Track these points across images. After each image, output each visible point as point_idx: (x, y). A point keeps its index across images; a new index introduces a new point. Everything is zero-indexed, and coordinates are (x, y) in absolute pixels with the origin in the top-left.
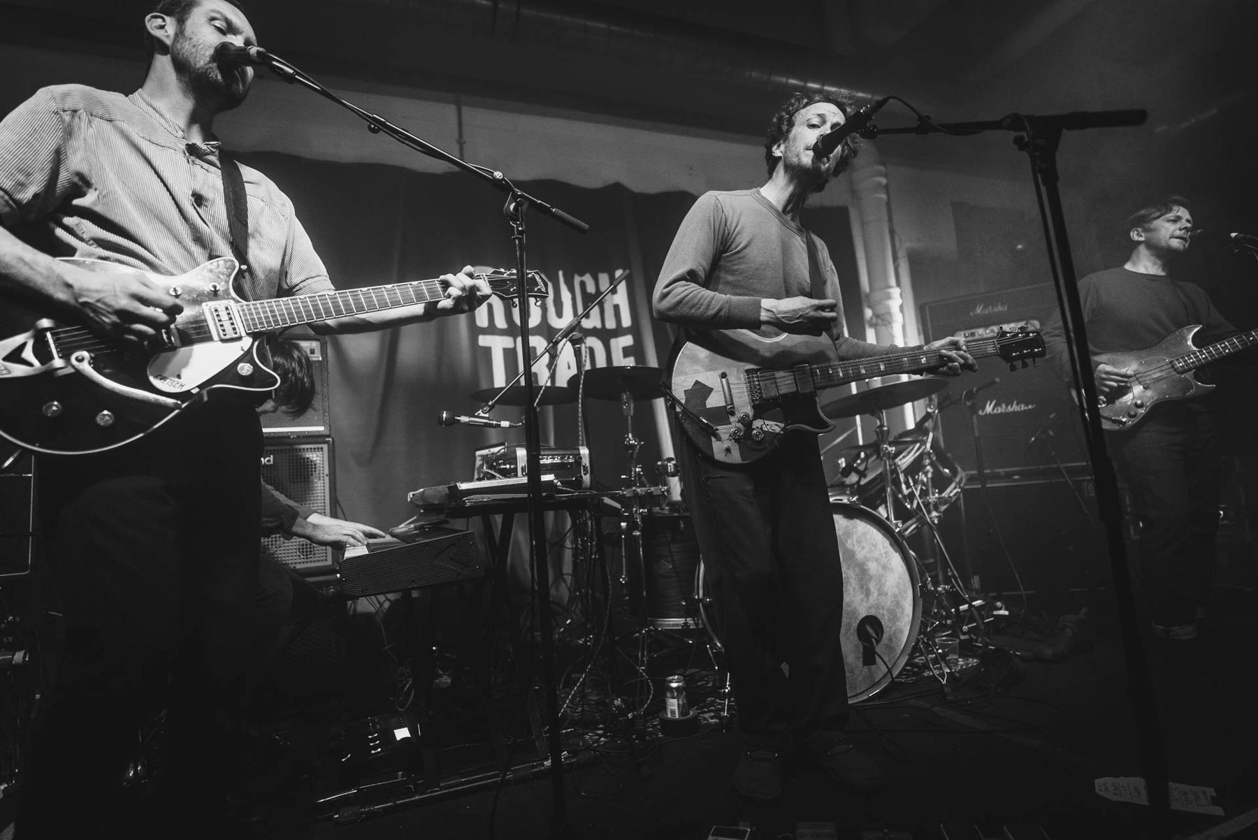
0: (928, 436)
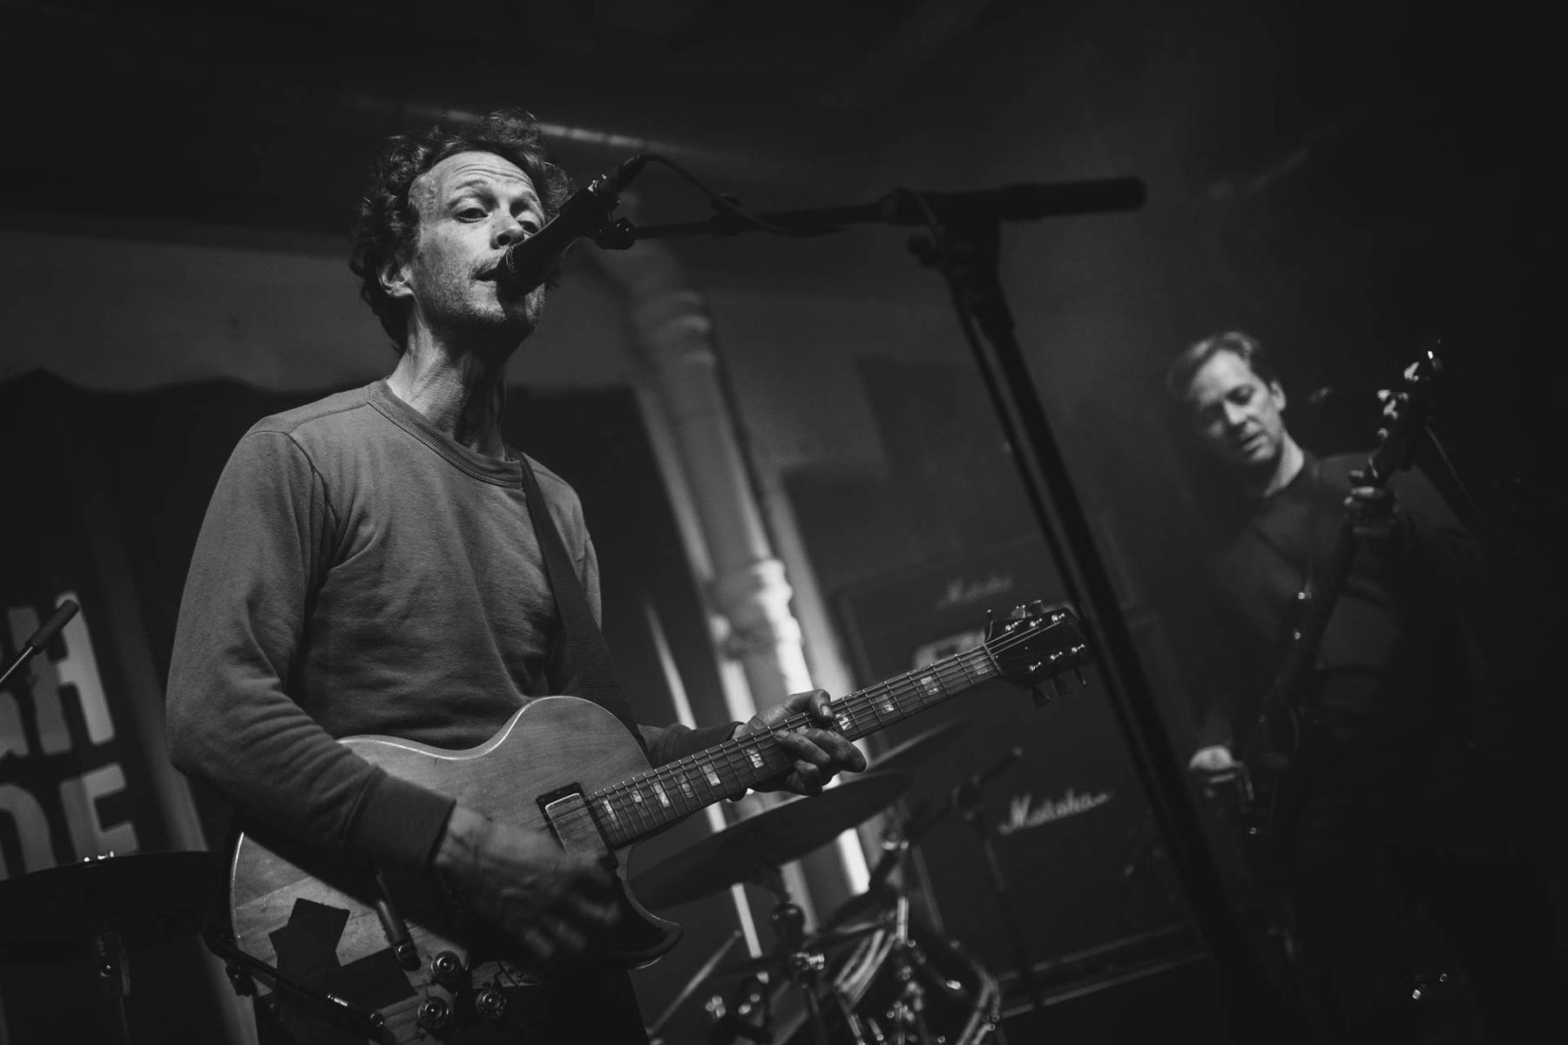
0: (895, 906)
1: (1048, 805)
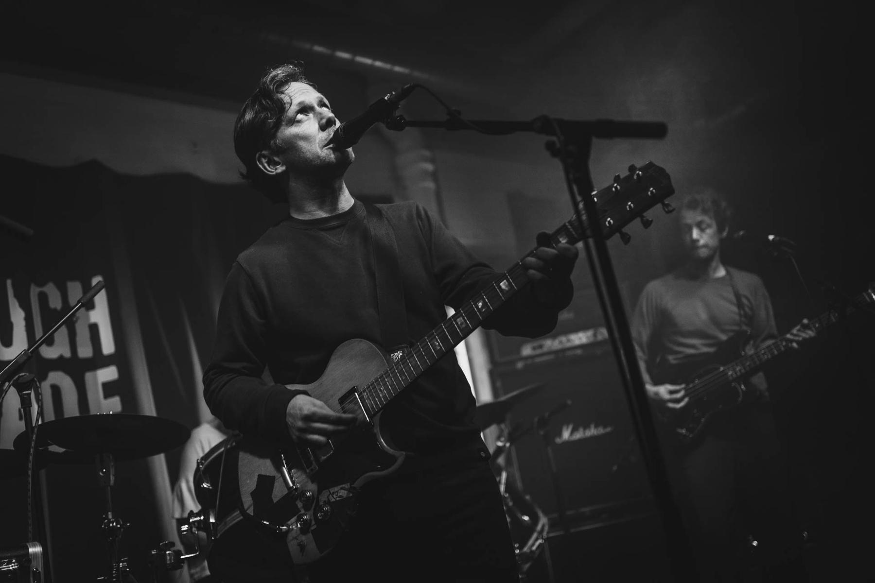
0: (500, 475)
1: (581, 430)
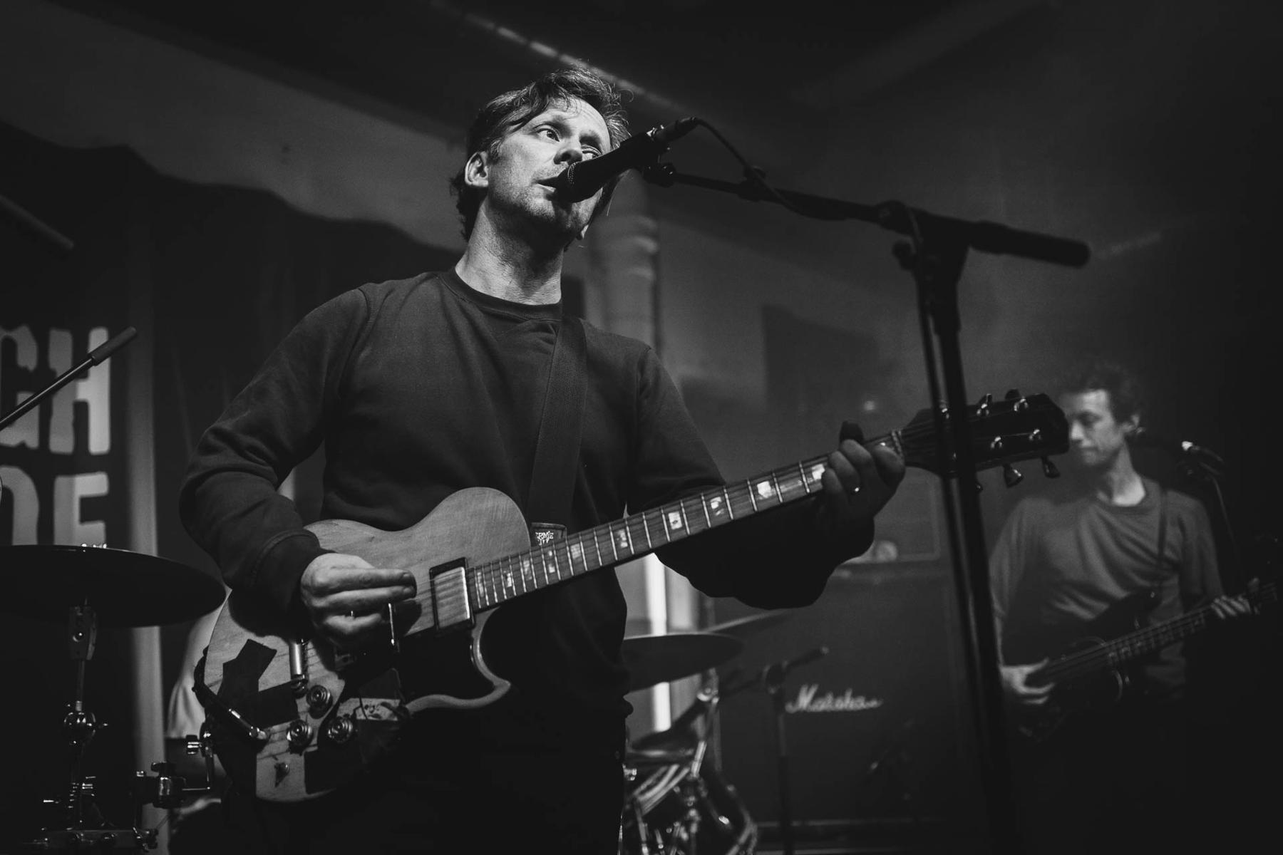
0: (695, 747)
